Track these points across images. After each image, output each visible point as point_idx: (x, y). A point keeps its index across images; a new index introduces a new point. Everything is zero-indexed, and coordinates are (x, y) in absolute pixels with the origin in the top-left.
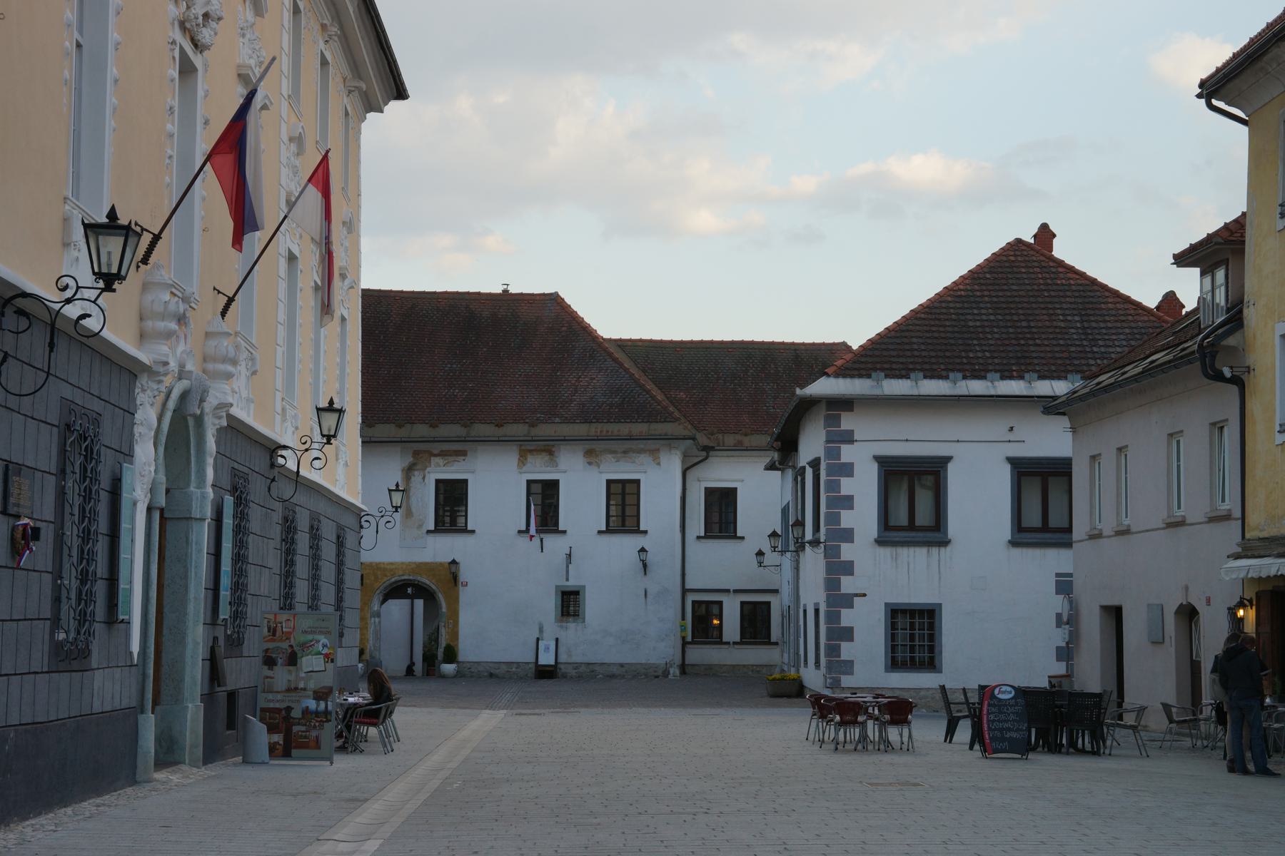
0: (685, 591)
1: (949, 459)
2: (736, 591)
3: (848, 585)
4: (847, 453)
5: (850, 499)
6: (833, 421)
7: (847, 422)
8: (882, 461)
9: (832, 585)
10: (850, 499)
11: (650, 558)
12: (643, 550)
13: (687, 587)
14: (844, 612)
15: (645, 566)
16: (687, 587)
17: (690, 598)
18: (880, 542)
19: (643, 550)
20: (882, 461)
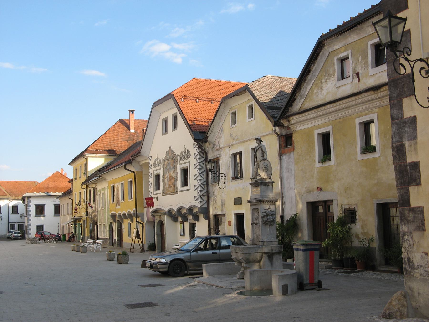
0: (9, 223)
1: (45, 204)
2: (18, 222)
3: (30, 222)
4: (30, 204)
5: (31, 210)
6: (28, 199)
7: (30, 199)
8: (35, 205)
9: (28, 222)
10: (31, 210)
11: (2, 218)
12: (1, 217)
13: (9, 222)
14: (30, 226)
15: (2, 219)
16: (9, 222)
17: (10, 224)
18: (35, 216)
19: (1, 217)
20: (35, 205)
